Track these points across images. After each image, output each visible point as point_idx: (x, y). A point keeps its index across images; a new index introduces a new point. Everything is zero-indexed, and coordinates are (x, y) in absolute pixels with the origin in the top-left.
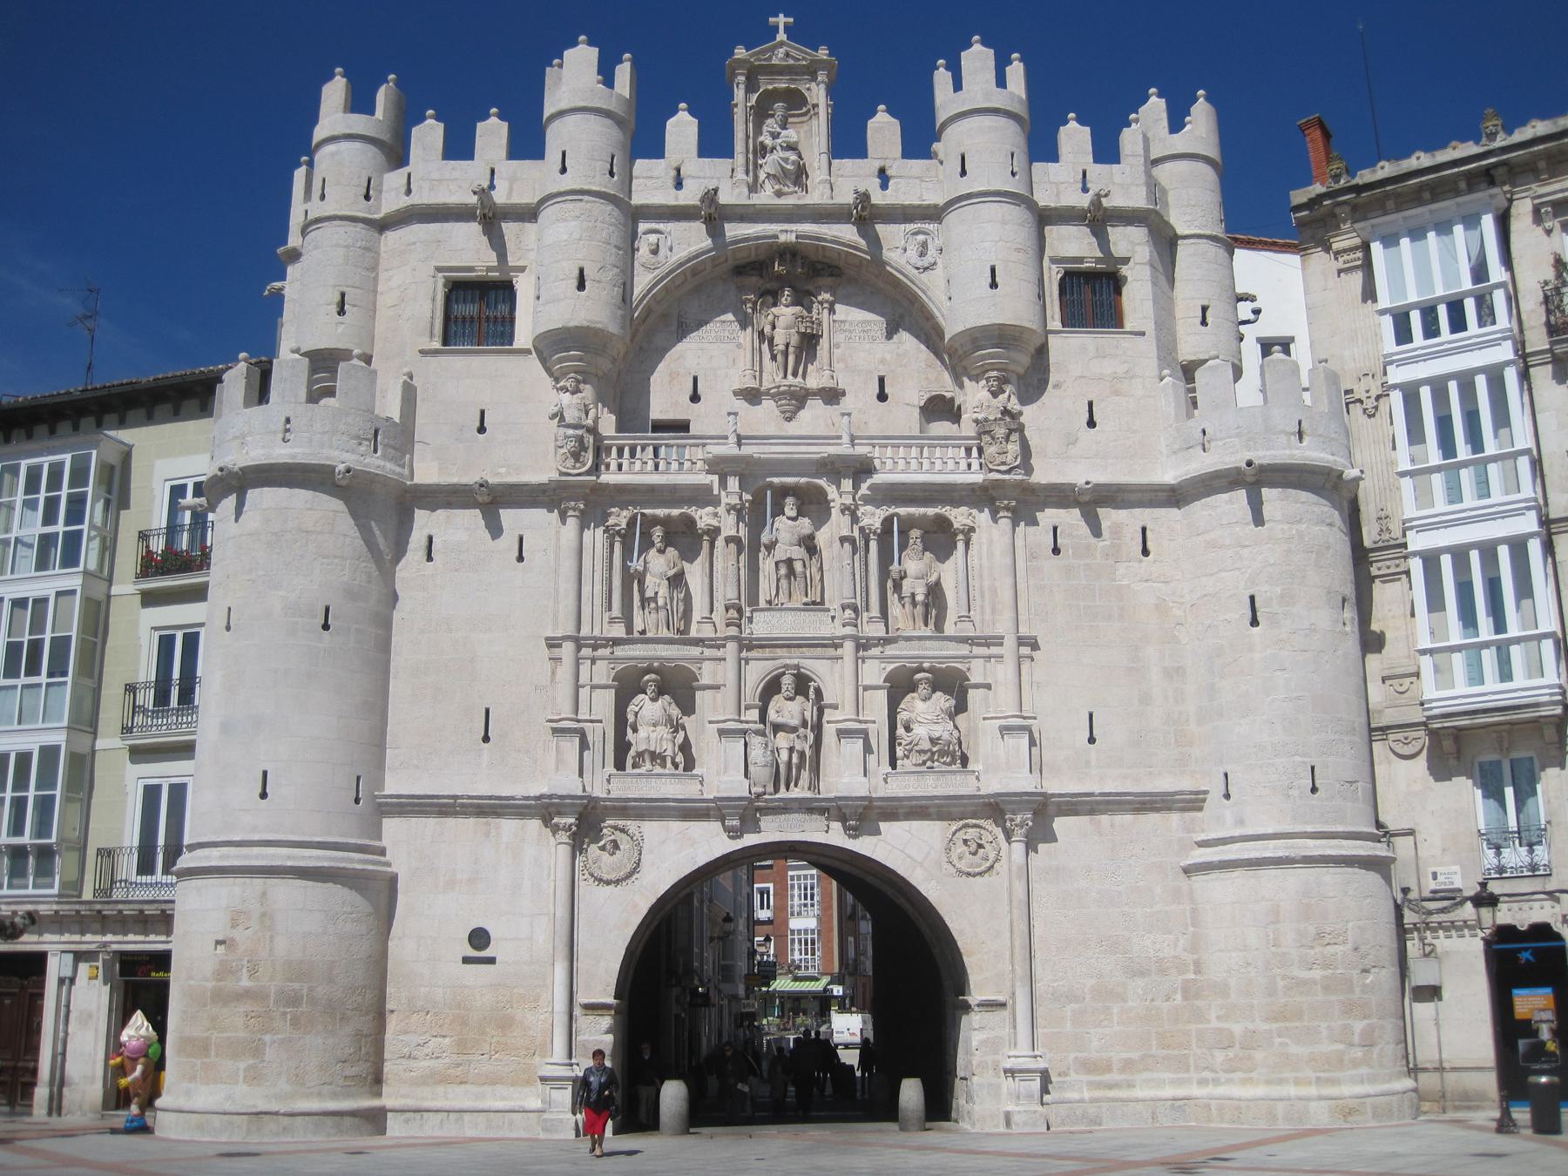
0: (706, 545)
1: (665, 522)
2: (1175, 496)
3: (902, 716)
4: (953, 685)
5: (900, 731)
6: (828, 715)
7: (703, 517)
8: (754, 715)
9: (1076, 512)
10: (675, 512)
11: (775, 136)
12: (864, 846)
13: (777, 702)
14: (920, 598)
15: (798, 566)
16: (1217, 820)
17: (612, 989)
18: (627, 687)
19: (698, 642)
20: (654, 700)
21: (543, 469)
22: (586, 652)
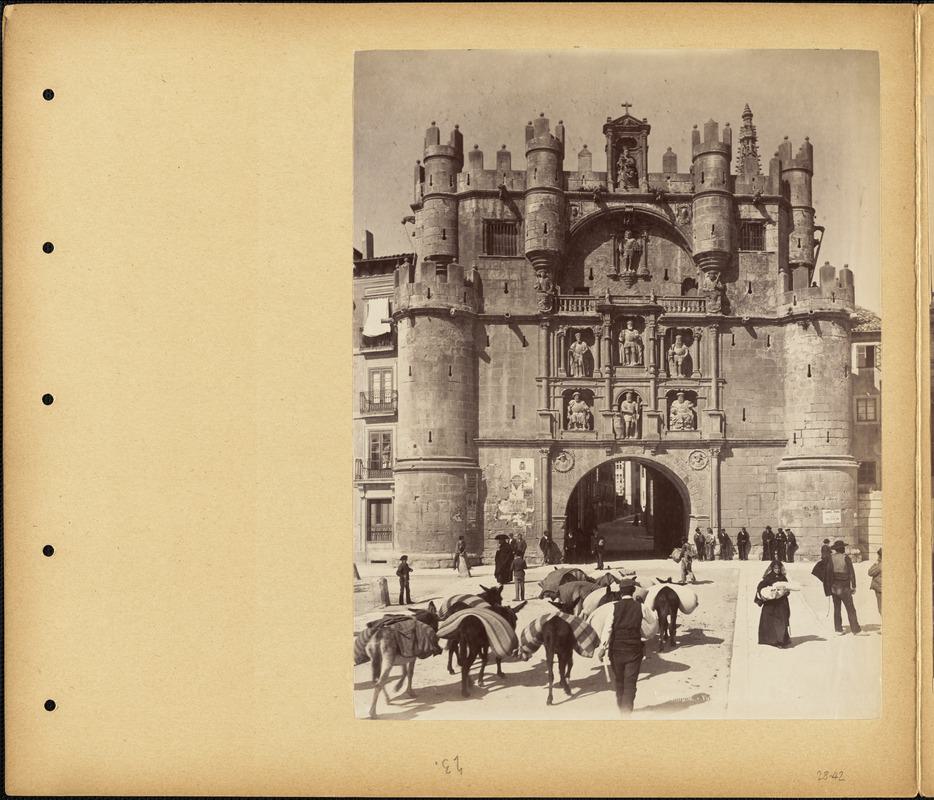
0: (596, 341)
1: (581, 331)
2: (781, 322)
3: (672, 410)
4: (691, 396)
5: (672, 415)
6: (644, 409)
7: (596, 329)
8: (615, 409)
9: (743, 328)
10: (585, 327)
11: (624, 161)
12: (659, 458)
13: (625, 403)
14: (680, 363)
15: (633, 349)
16: (791, 450)
17: (564, 511)
18: (567, 396)
19: (595, 380)
20: (578, 402)
21: (537, 308)
22: (552, 384)
